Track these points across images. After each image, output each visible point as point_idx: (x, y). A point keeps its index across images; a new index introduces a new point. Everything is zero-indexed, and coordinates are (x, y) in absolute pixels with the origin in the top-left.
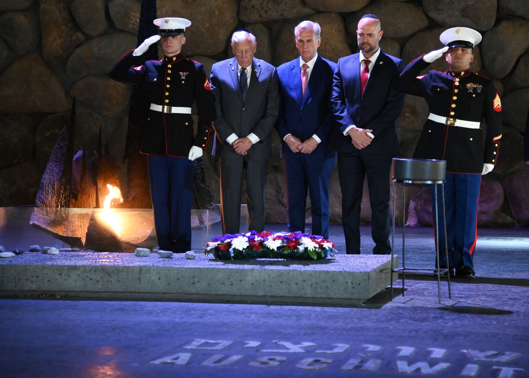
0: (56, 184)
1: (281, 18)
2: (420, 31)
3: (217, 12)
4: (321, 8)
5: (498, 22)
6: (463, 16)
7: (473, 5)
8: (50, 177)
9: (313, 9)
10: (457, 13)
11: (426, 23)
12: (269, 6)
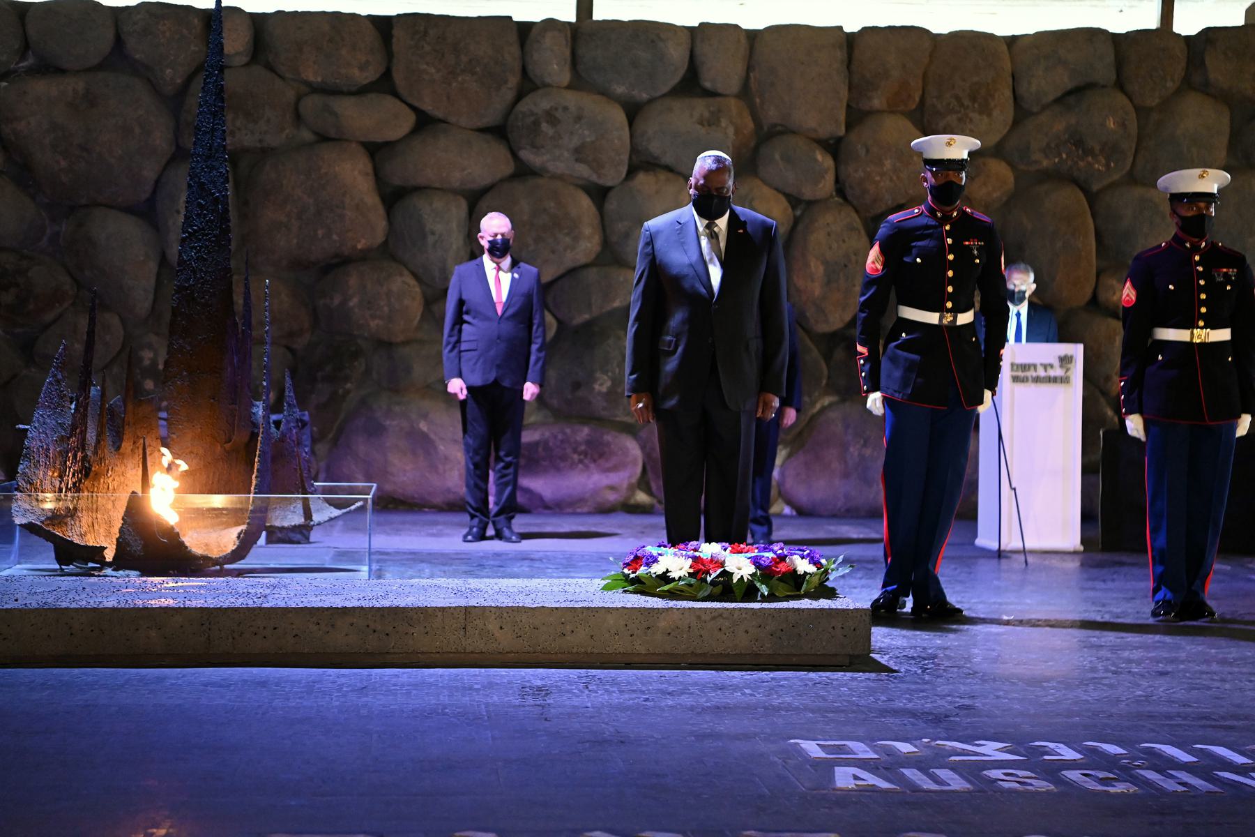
0: (51, 448)
1: (259, 145)
2: (502, 181)
3: (137, 130)
4: (332, 133)
5: (632, 172)
6: (577, 160)
7: (593, 142)
8: (40, 431)
9: (316, 133)
10: (566, 154)
11: (507, 168)
12: (238, 123)
